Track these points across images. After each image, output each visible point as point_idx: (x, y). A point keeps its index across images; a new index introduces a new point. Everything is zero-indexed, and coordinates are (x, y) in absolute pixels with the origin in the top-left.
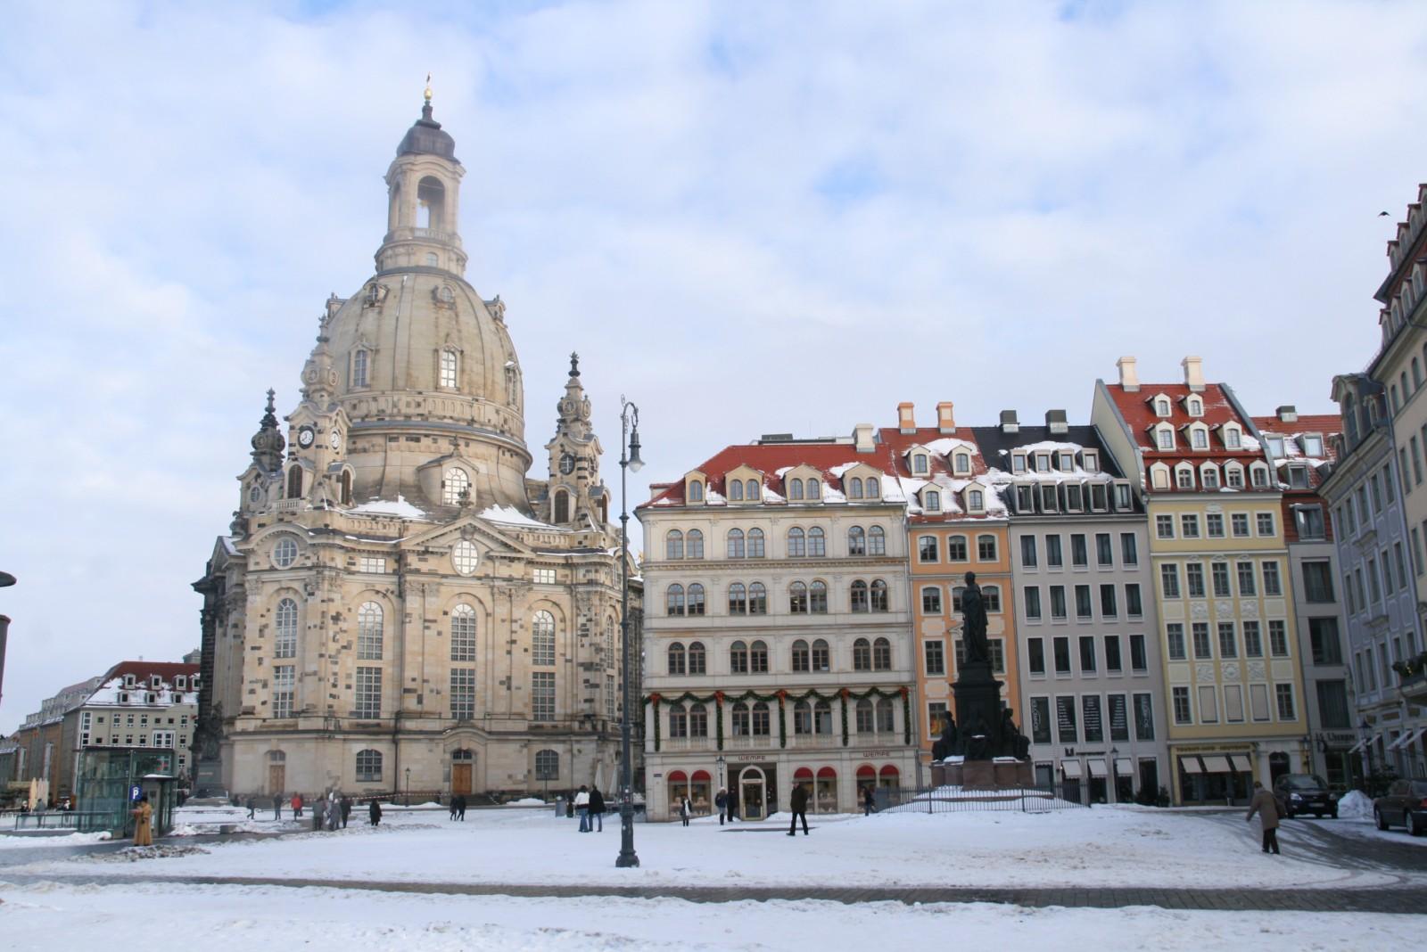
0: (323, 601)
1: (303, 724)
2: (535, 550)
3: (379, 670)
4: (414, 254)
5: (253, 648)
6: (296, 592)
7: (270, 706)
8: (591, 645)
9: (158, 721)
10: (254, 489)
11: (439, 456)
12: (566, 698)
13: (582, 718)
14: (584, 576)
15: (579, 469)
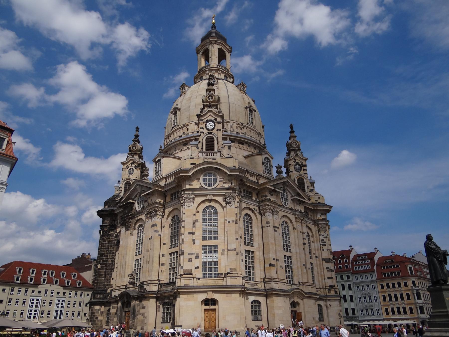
0: (236, 208)
1: (229, 282)
2: (309, 199)
3: (253, 252)
4: (220, 74)
5: (190, 233)
6: (216, 201)
7: (200, 269)
8: (328, 250)
9: (33, 292)
10: (130, 169)
11: (251, 153)
12: (318, 276)
13: (329, 288)
14: (321, 216)
15: (304, 170)
